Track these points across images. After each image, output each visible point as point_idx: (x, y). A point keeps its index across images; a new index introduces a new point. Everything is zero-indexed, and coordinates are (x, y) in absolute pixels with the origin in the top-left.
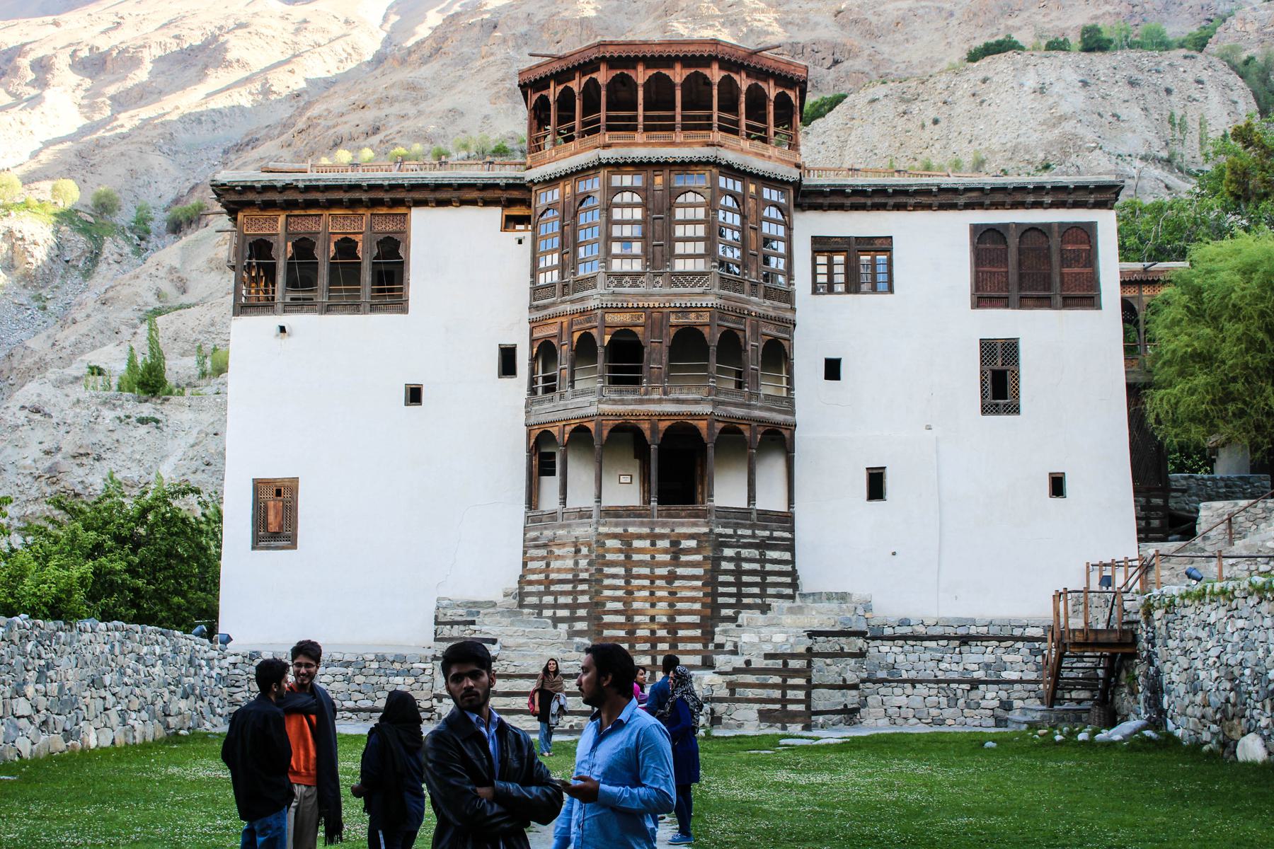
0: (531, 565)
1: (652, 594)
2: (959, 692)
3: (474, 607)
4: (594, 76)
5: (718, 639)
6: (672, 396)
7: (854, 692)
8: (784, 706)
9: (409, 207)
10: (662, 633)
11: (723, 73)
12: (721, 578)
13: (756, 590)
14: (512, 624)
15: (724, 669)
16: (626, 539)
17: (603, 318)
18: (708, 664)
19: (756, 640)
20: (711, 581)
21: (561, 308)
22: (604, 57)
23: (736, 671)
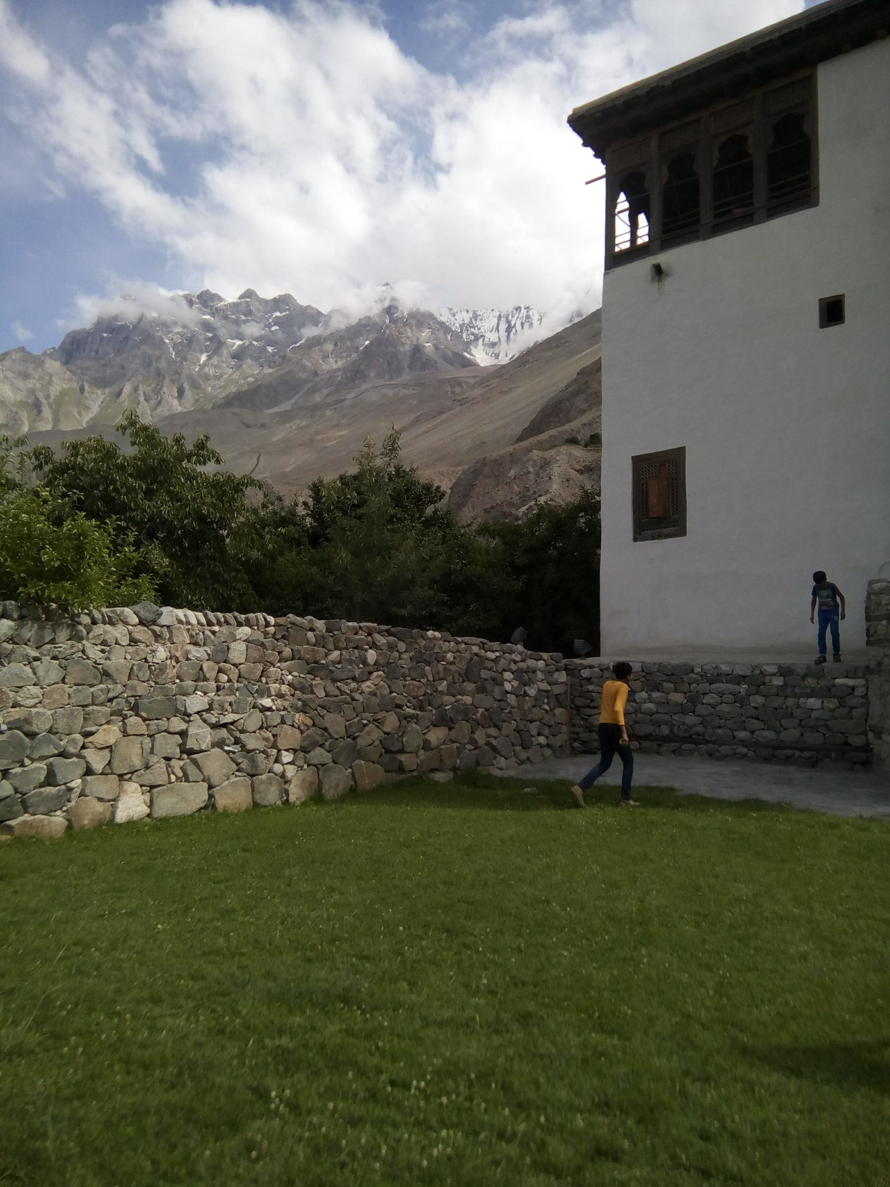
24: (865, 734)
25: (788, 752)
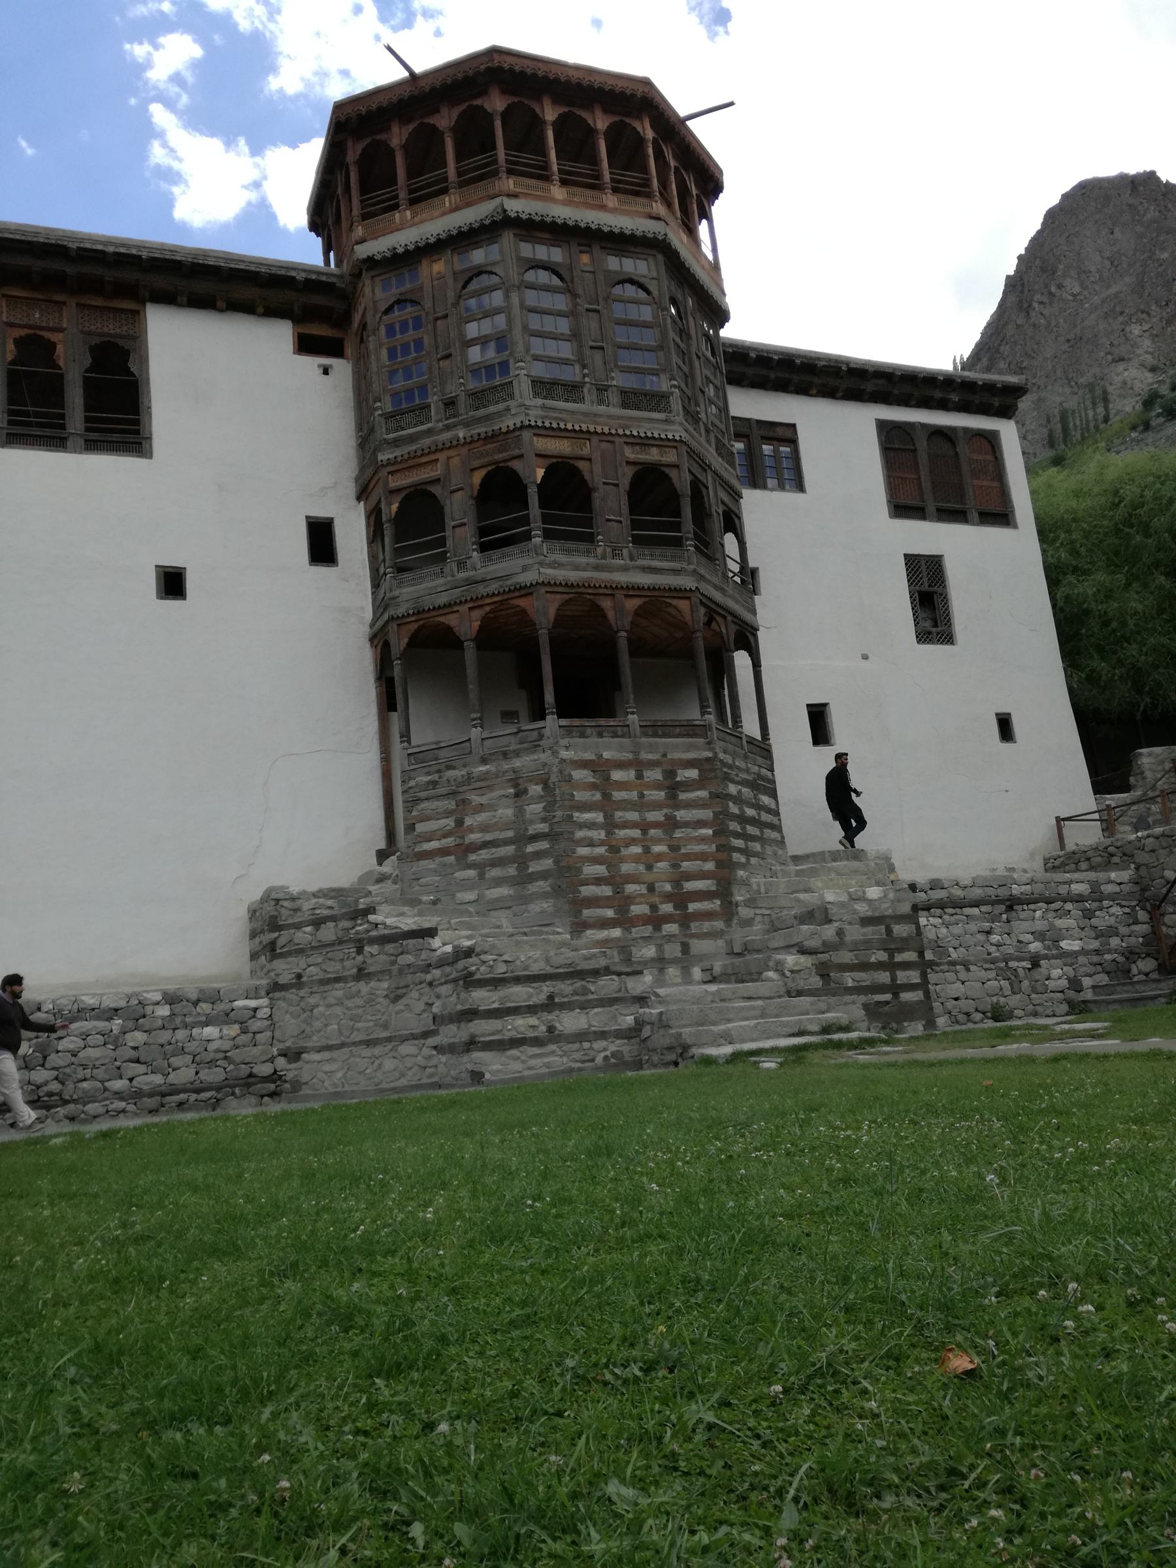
0: (420, 828)
1: (647, 850)
2: (1021, 972)
4: (478, 102)
5: (744, 912)
6: (640, 562)
8: (896, 995)
9: (143, 303)
10: (667, 908)
17: (531, 442)
19: (844, 898)
23: (828, 947)
24: (272, 1060)
25: (183, 1096)
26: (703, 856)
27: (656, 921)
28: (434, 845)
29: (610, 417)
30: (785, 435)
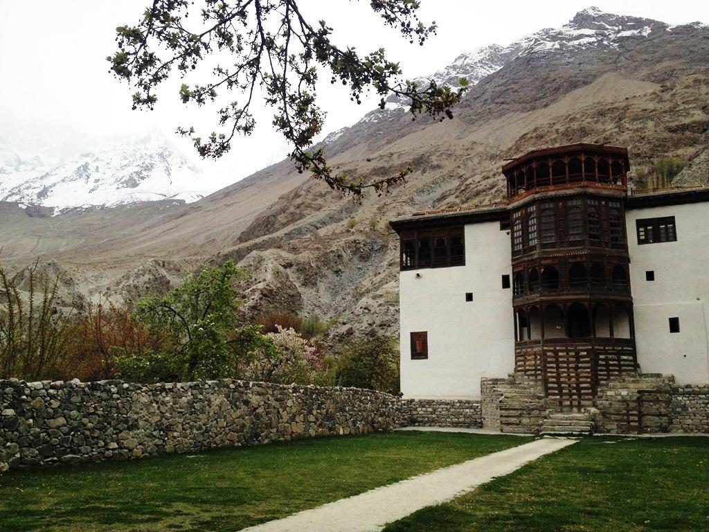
1: (569, 375)
3: (495, 381)
5: (599, 394)
6: (571, 292)
7: (666, 418)
10: (574, 391)
11: (586, 157)
12: (599, 368)
13: (617, 373)
14: (511, 388)
15: (601, 407)
16: (556, 352)
17: (540, 263)
18: (595, 405)
19: (614, 394)
20: (594, 370)
21: (523, 259)
22: (534, 157)
26: (587, 377)
27: (571, 395)
28: (520, 368)
29: (565, 251)
30: (671, 220)
